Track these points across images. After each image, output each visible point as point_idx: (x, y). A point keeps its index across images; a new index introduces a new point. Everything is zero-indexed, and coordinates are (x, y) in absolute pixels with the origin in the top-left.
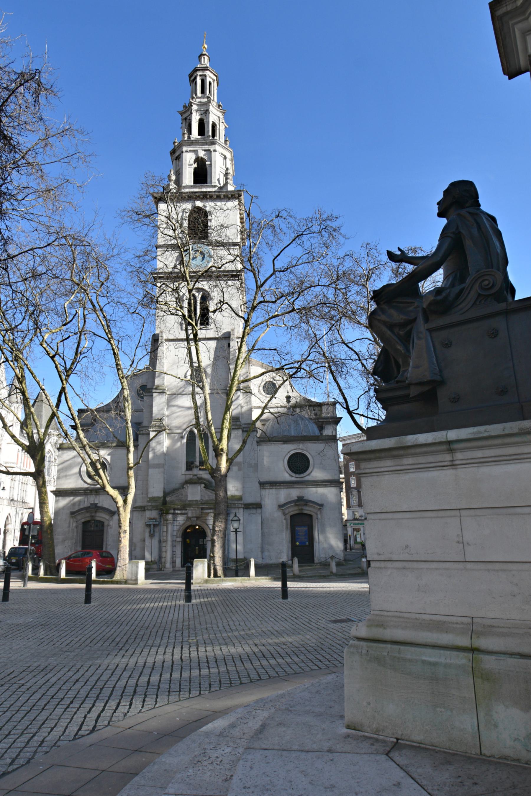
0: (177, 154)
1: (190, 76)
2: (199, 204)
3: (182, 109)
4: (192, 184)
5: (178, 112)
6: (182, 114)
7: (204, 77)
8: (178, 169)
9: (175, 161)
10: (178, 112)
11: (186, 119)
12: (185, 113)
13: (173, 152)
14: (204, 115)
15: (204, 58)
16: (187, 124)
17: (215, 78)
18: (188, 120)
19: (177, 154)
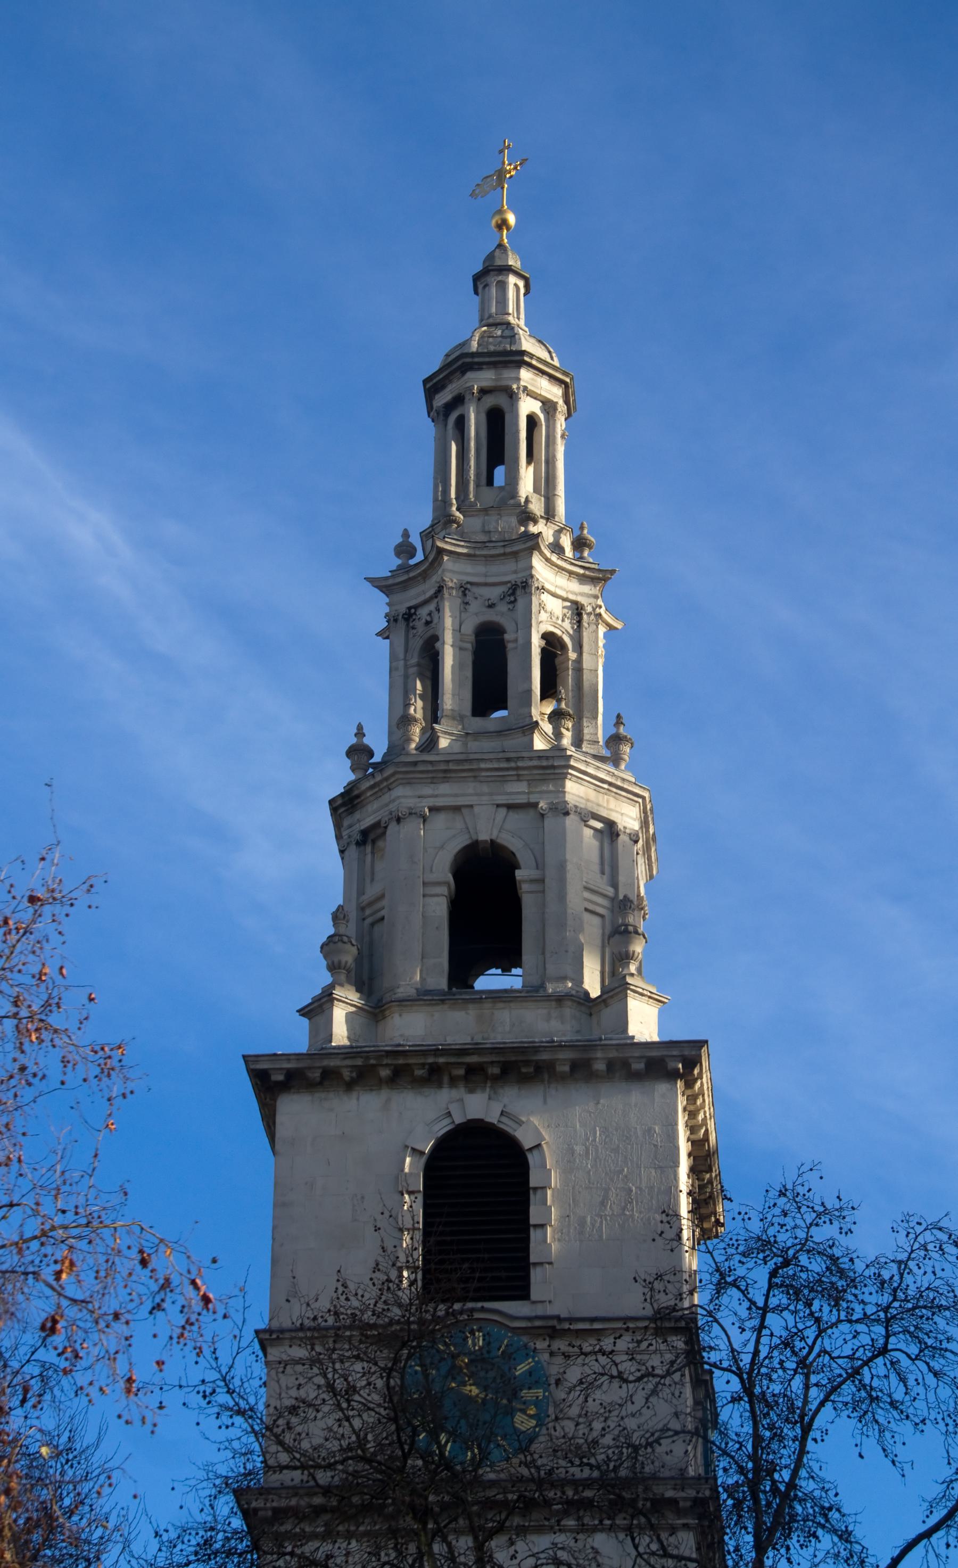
0: (366, 818)
1: (433, 386)
2: (478, 1106)
3: (388, 564)
4: (443, 983)
5: (370, 580)
6: (385, 586)
7: (500, 400)
8: (372, 891)
9: (353, 851)
10: (370, 580)
11: (409, 616)
12: (405, 585)
13: (345, 805)
14: (503, 607)
15: (503, 286)
16: (417, 644)
17: (554, 393)
18: (419, 625)
19: (366, 818)
